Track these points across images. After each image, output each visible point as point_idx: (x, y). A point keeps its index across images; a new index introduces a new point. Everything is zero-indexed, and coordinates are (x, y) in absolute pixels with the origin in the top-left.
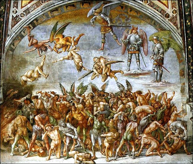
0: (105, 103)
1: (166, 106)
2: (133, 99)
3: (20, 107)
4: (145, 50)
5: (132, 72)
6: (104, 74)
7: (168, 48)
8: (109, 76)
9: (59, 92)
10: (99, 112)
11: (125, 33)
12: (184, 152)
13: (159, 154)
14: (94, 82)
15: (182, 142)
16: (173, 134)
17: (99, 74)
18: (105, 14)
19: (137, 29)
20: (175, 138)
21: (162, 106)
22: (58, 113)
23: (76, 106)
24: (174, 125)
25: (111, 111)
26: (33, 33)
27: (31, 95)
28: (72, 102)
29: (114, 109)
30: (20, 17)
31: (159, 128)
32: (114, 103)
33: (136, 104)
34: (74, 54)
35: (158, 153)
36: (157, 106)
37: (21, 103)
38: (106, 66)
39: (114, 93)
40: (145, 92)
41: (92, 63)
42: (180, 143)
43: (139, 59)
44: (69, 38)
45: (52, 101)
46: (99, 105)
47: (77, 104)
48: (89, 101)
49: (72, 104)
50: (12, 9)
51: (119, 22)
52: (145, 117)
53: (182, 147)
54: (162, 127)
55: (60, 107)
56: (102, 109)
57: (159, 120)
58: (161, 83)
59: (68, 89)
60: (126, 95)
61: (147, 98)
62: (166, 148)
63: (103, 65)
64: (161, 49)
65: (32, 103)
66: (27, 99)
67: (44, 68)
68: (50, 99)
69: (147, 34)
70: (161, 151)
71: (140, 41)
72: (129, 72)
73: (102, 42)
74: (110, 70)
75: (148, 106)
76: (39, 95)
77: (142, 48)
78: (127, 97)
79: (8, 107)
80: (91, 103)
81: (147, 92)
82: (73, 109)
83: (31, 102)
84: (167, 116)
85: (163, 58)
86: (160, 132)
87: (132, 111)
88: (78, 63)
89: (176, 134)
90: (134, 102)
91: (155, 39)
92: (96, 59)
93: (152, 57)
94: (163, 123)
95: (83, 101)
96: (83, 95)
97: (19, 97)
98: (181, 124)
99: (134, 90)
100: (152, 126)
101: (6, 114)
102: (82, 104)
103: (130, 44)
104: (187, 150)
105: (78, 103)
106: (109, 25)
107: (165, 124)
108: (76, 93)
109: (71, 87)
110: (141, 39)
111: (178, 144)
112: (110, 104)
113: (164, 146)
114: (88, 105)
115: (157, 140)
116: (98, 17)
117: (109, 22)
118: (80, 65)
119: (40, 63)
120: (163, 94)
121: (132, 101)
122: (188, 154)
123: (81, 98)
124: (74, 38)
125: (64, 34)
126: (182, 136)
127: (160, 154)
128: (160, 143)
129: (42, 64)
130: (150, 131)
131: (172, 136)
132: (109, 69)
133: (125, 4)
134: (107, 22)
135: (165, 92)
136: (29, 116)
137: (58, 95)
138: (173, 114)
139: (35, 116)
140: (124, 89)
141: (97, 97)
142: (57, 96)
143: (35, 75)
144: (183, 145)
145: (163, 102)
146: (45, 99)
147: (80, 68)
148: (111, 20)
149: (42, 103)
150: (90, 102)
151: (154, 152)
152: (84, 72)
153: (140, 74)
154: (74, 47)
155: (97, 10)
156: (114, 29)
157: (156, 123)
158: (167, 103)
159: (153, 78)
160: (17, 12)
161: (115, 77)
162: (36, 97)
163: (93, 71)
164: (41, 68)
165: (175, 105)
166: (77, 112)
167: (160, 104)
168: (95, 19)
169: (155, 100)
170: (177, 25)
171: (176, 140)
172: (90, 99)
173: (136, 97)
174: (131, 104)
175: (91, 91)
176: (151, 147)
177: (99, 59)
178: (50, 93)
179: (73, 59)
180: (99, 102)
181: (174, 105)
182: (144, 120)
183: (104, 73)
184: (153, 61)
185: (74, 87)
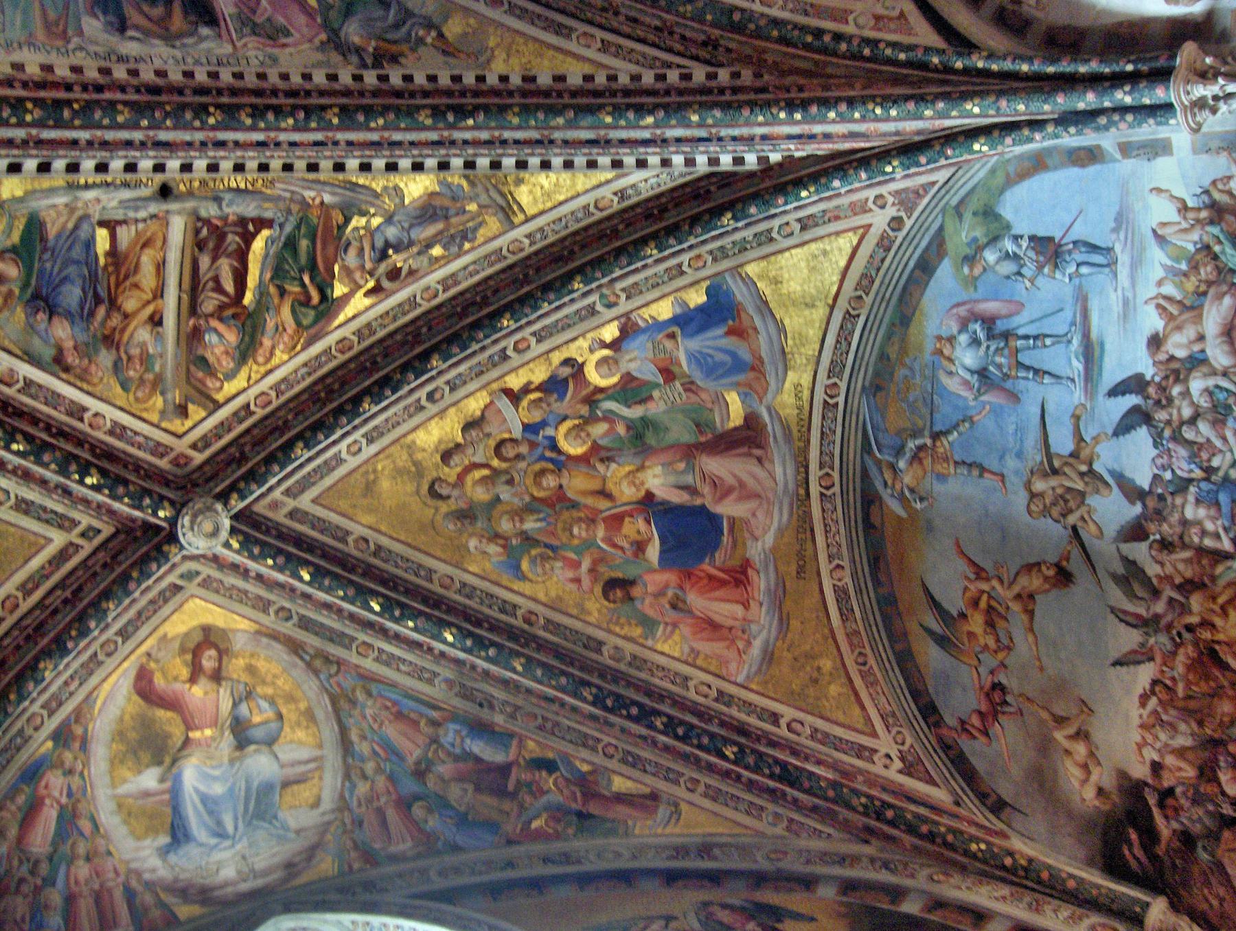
0: (1191, 498)
1: (1209, 229)
2: (1176, 373)
3: (1187, 839)
4: (1004, 312)
5: (1078, 365)
6: (1086, 484)
7: (998, 217)
8: (1091, 465)
9: (1145, 674)
10: (1226, 530)
11: (952, 384)
14: (1111, 530)
17: (1083, 503)
18: (899, 451)
19: (939, 338)
21: (1207, 247)
22: (1220, 698)
23: (1194, 620)
25: (1221, 473)
26: (951, 721)
27: (1146, 784)
28: (1179, 634)
29: (1215, 463)
30: (905, 748)
32: (1193, 457)
33: (1197, 361)
34: (1016, 589)
36: (1209, 269)
37: (1174, 831)
38: (1055, 472)
39: (1155, 452)
40: (1153, 322)
41: (1047, 524)
43: (1036, 338)
44: (968, 595)
45: (1173, 712)
46: (1199, 523)
47: (1190, 612)
48: (1179, 564)
49: (1187, 635)
50: (877, 769)
51: (920, 404)
55: (1197, 684)
56: (1213, 512)
58: (1118, 248)
59: (1130, 638)
60: (1164, 402)
61: (1175, 312)
63: (1054, 482)
64: (999, 245)
65: (1179, 790)
66: (1161, 805)
67: (1060, 710)
68: (1164, 717)
69: (955, 300)
71: (977, 327)
72: (1080, 383)
73: (981, 476)
74: (1071, 460)
75: (1206, 308)
76: (1150, 754)
77: (1001, 326)
78: (1170, 400)
79: (1185, 884)
80: (1187, 554)
81: (1151, 309)
82: (1206, 635)
83: (1170, 792)
85: (1032, 238)
87: (1224, 383)
88: (1046, 579)
90: (1190, 370)
91: (971, 268)
92: (1033, 508)
93: (1028, 284)
95: (1179, 588)
96: (1155, 581)
97: (1150, 835)
99: (1146, 367)
101: (1207, 900)
102: (1191, 592)
103: (985, 369)
105: (1185, 609)
106: (929, 442)
108: (1148, 610)
109: (1128, 624)
112: (1193, 475)
114: (1196, 566)
116: (908, 479)
117: (919, 442)
118: (1051, 573)
119: (1042, 722)
120: (1160, 239)
121: (1186, 381)
123: (1169, 592)
124: (967, 578)
125: (955, 613)
129: (1045, 715)
132: (1066, 464)
134: (921, 448)
135: (1154, 231)
136: (1222, 815)
137: (1155, 682)
139: (1223, 793)
140: (1135, 410)
141: (1165, 527)
142: (1157, 689)
143: (1080, 749)
145: (1189, 244)
146: (1163, 736)
147: (1063, 577)
148: (915, 434)
149: (1181, 753)
150: (1187, 561)
152: (1076, 564)
153: (1086, 336)
154: (995, 583)
155: (888, 475)
156: (937, 428)
158: (1198, 221)
159: (1103, 277)
160: (888, 756)
161: (1096, 439)
162: (1156, 767)
163: (1074, 528)
164: (1060, 721)
165: (1206, 183)
166: (1218, 621)
167: (1198, 257)
168: (912, 491)
169: (1185, 275)
170: (923, 186)
172: (1174, 557)
173: (1172, 358)
174: (1197, 385)
175: (1144, 546)
177: (1033, 496)
178: (1145, 713)
179: (1031, 597)
180: (1185, 523)
181: (1207, 192)
183: (1080, 486)
184: (1040, 281)
185: (1125, 612)
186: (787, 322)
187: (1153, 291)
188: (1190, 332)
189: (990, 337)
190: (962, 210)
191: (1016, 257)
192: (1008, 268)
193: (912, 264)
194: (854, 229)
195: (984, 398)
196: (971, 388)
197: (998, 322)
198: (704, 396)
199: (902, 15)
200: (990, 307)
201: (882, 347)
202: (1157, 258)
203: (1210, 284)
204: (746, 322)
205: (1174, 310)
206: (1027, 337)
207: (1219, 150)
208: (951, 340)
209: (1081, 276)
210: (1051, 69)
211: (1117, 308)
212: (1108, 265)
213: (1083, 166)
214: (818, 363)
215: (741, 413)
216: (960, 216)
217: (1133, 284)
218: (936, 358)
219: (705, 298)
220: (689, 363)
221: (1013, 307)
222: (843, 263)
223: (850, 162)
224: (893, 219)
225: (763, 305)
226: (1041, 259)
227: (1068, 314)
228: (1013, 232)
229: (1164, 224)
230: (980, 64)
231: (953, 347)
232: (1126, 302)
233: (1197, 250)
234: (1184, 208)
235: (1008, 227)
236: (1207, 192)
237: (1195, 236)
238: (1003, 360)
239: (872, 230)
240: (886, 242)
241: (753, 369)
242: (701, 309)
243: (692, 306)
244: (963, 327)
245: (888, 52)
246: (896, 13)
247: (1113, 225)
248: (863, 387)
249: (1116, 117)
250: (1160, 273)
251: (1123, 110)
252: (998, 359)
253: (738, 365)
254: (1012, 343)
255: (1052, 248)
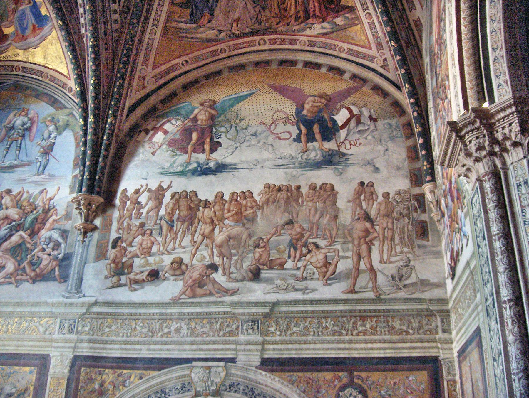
1: (42, 209)
5: (7, 164)
7: (64, 129)
11: (11, 116)
12: (54, 279)
13: (14, 282)
15: (54, 263)
16: (44, 250)
20: (46, 256)
21: (36, 209)
24: (47, 237)
31: (24, 242)
35: (13, 280)
36: (29, 210)
42: (50, 265)
43: (20, 147)
52: (8, 226)
53: (52, 270)
54: (28, 240)
57: (27, 229)
58: (43, 176)
62: (25, 272)
64: (55, 131)
69: (39, 116)
70: (19, 277)
71: (29, 125)
75: (16, 209)
77: (27, 133)
81: (20, 189)
84: (40, 223)
85: (54, 143)
86: (23, 247)
89: (47, 250)
94: (33, 233)
98: (59, 235)
100: (15, 238)
104: (60, 275)
107: (34, 235)
110: (29, 122)
111: (47, 265)
113: (24, 268)
115: (16, 260)
120: (42, 192)
122: (60, 282)
126: (56, 253)
127: (15, 281)
128: (19, 265)
130: (9, 246)
131: (41, 254)
133: (21, 83)
135: (45, 189)
138: (51, 220)
144: (55, 268)
151: (8, 278)
157: (21, 235)
158: (45, 205)
159: (35, 171)
165: (57, 207)
169: (29, 201)
171: (46, 259)
176: (4, 271)
181: (54, 207)
182: (6, 229)
186: (39, 48)
187: (25, 190)
188: (9, 204)
189: (24, 130)
190: (71, 115)
191: (49, 137)
192: (46, 135)
193: (57, 97)
194: (69, 74)
195: (4, 130)
196: (8, 124)
197: (28, 133)
198: (12, 17)
199: (145, 87)
200: (34, 129)
201: (31, 87)
202: (34, 190)
203: (24, 210)
204: (38, 32)
205: (17, 198)
206: (21, 144)
207: (67, 211)
208: (27, 115)
209: (37, 163)
210: (103, 148)
211: (23, 177)
212: (38, 173)
213: (74, 161)
214: (26, 62)
215: (8, 33)
216: (68, 115)
217: (30, 182)
218: (21, 109)
219: (44, 14)
220: (22, 10)
221: (32, 138)
222: (58, 70)
223: (81, 72)
224: (72, 89)
225: (43, 39)
226: (46, 147)
227: (25, 159)
228: (58, 136)
229: (47, 193)
230: (109, 120)
231: (23, 116)
232: (24, 180)
233: (35, 205)
234: (50, 199)
235: (60, 134)
236: (54, 207)
237: (40, 204)
238: (15, 135)
239: (68, 81)
240: (65, 86)
241: (23, 36)
242: (40, 13)
243: (41, 10)
244: (30, 119)
245: (118, 84)
246: (146, 85)
247: (51, 174)
248: (18, 81)
249: (81, 173)
250: (31, 192)
251: (83, 176)
252: (16, 133)
253: (23, 30)
254: (20, 138)
255: (48, 151)
